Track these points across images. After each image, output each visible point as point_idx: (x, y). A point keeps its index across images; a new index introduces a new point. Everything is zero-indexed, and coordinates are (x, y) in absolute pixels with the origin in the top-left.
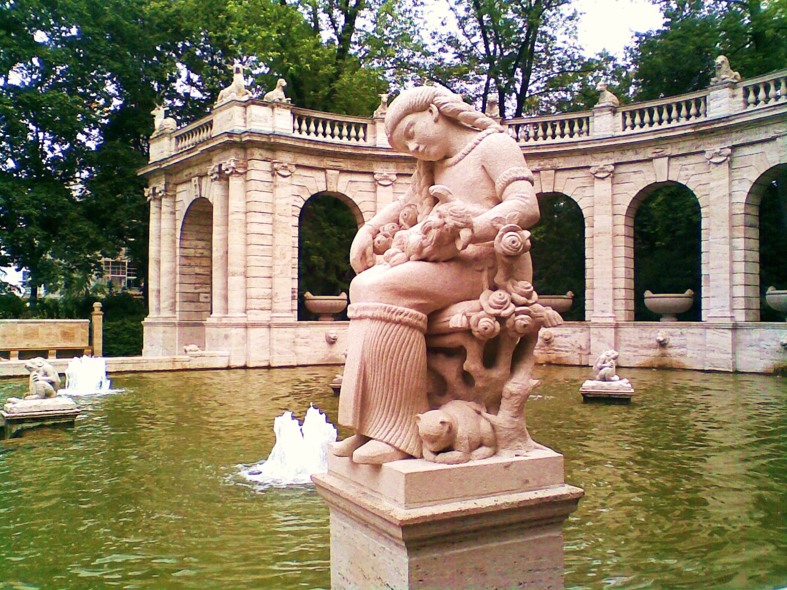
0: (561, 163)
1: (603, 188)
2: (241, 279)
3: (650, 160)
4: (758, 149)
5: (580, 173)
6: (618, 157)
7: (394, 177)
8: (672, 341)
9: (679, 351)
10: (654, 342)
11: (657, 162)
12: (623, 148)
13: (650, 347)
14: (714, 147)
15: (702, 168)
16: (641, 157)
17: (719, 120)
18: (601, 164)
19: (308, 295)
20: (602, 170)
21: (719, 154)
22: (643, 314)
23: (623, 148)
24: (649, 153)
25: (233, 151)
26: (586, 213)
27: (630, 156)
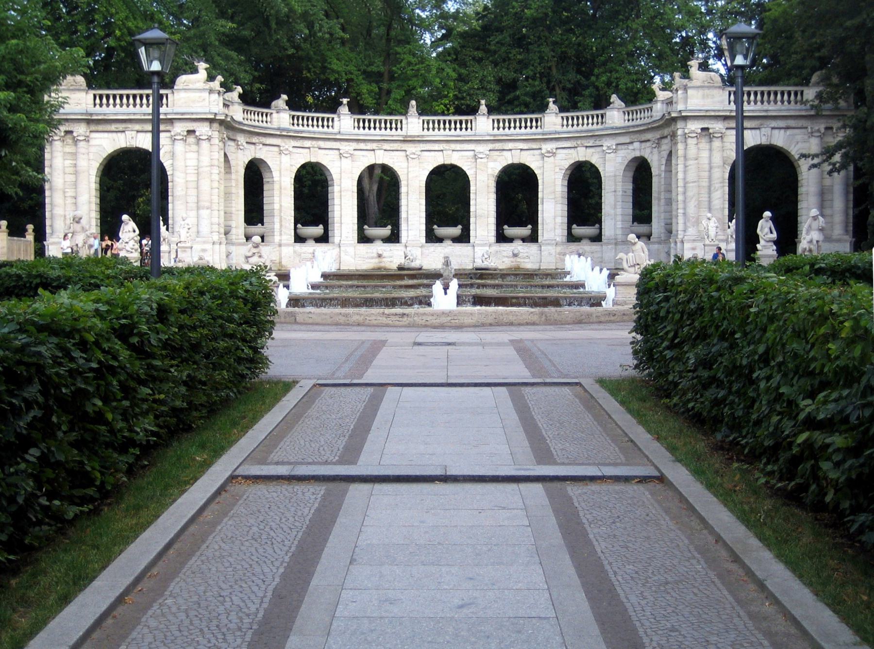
0: (322, 144)
1: (346, 163)
3: (374, 150)
6: (354, 145)
7: (244, 144)
8: (385, 254)
9: (389, 260)
10: (375, 255)
13: (372, 258)
14: (411, 148)
16: (368, 148)
17: (418, 136)
18: (347, 148)
19: (299, 226)
20: (347, 152)
21: (414, 154)
22: (363, 239)
23: (358, 141)
24: (374, 146)
26: (334, 177)
27: (362, 146)
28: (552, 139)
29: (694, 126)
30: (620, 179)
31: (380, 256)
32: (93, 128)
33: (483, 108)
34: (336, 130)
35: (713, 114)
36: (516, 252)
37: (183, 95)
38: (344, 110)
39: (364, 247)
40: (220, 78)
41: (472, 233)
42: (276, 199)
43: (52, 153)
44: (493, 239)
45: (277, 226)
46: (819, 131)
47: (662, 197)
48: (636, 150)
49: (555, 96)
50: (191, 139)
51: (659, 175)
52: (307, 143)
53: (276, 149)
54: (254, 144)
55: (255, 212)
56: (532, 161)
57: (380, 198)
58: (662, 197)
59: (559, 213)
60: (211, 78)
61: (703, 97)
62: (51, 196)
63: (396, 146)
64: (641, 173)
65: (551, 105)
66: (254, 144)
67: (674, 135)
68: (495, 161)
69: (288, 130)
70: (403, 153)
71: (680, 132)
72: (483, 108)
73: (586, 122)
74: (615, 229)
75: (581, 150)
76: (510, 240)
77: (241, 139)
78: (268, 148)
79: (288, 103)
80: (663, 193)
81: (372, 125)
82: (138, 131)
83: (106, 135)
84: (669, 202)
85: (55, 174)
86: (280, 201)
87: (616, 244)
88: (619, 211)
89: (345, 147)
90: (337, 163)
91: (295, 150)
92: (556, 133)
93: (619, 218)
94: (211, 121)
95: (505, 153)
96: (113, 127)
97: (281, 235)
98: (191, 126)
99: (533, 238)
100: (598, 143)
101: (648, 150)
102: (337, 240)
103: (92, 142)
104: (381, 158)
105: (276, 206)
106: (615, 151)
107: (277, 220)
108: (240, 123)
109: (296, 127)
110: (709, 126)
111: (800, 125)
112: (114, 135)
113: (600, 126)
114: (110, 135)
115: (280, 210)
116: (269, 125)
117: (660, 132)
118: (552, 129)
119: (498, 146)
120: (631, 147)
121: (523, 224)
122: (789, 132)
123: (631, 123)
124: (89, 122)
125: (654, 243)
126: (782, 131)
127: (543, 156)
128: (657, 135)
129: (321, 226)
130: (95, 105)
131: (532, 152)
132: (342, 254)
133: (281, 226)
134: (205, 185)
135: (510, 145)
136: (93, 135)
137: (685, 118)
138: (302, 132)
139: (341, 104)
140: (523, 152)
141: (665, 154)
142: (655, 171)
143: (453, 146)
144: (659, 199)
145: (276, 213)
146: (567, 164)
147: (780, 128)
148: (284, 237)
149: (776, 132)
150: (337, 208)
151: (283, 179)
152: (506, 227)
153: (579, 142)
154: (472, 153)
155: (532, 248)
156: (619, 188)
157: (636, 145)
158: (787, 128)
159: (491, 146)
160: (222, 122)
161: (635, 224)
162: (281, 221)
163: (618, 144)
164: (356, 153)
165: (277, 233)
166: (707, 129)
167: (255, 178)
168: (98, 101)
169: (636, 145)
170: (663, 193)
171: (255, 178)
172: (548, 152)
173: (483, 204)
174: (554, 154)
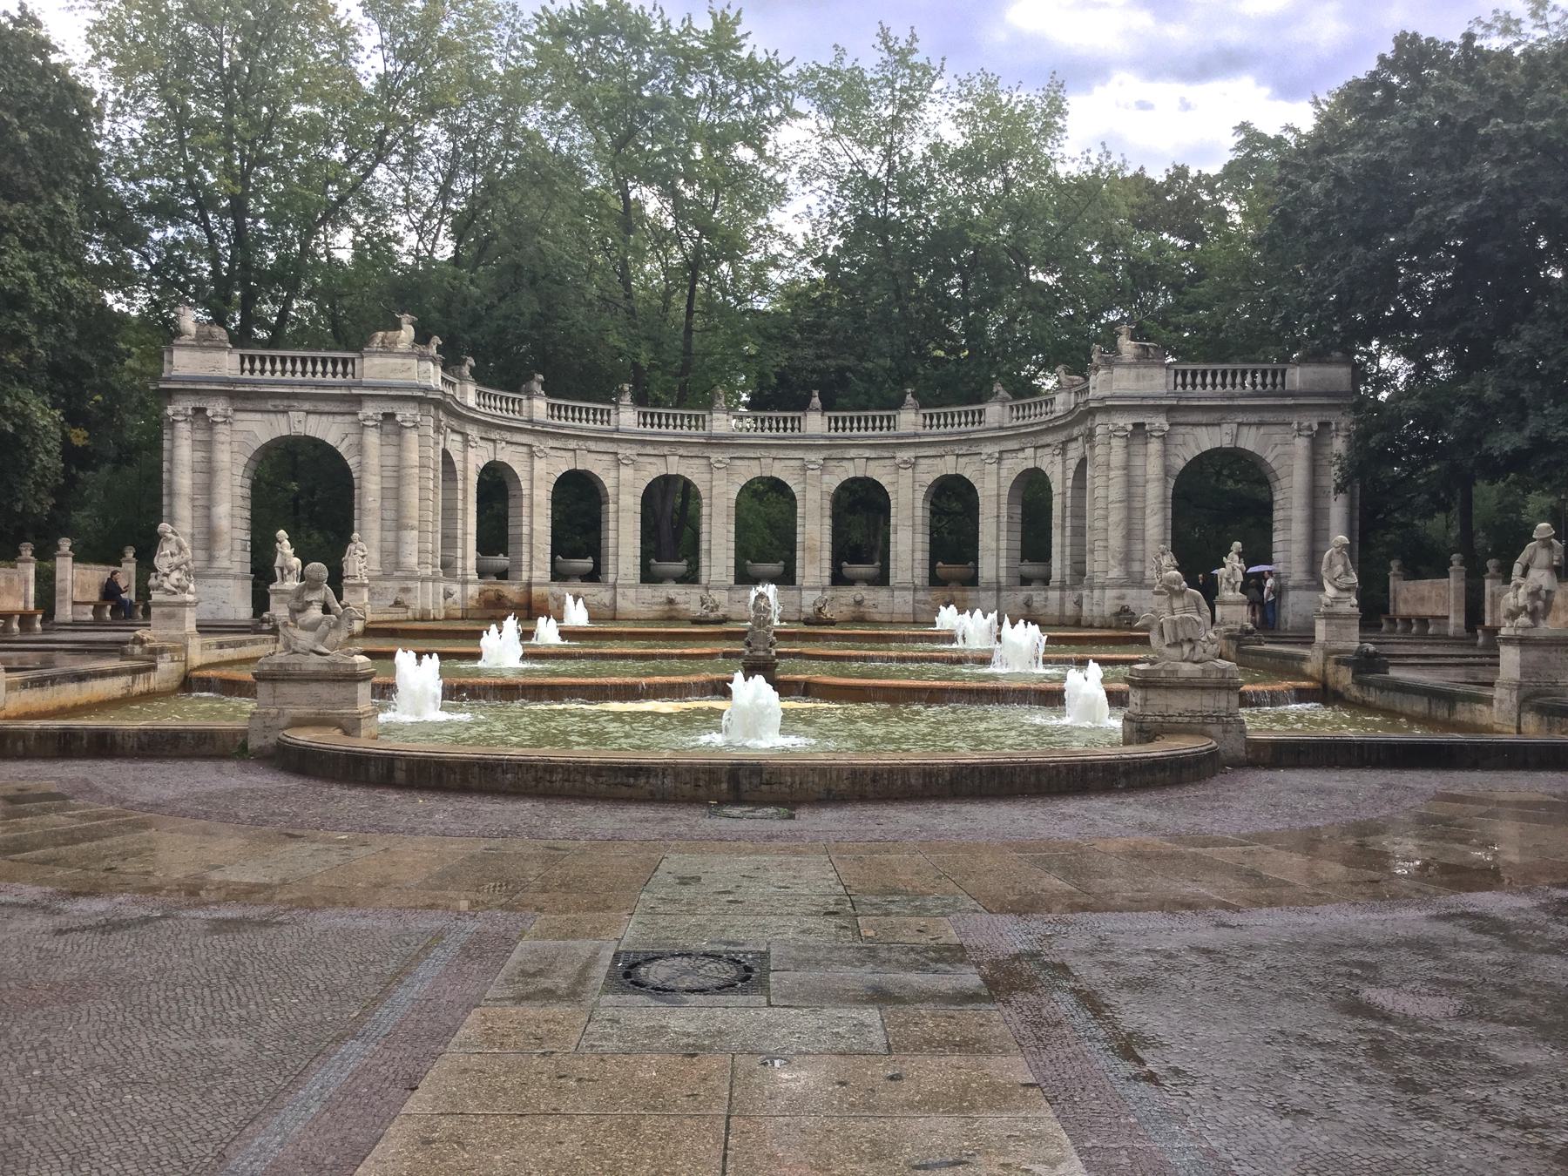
0: (592, 445)
2: (415, 533)
4: (746, 462)
5: (605, 457)
8: (678, 599)
11: (670, 459)
12: (643, 443)
14: (715, 455)
15: (703, 469)
18: (628, 452)
20: (627, 458)
23: (643, 443)
24: (666, 450)
25: (412, 405)
26: (610, 491)
27: (649, 450)
28: (909, 445)
29: (1126, 421)
30: (1004, 499)
31: (671, 601)
32: (239, 405)
33: (816, 401)
34: (612, 427)
35: (1152, 402)
36: (858, 598)
37: (377, 360)
38: (627, 399)
39: (648, 591)
40: (436, 340)
41: (799, 572)
42: (525, 520)
43: (172, 440)
44: (827, 581)
45: (525, 558)
46: (1310, 428)
47: (1068, 524)
48: (1026, 460)
49: (915, 384)
50: (388, 428)
51: (1064, 494)
52: (572, 444)
53: (525, 449)
54: (494, 441)
55: (496, 534)
56: (881, 473)
57: (671, 521)
58: (1068, 524)
59: (919, 546)
60: (422, 338)
61: (1138, 378)
62: (171, 505)
63: (695, 451)
64: (1032, 495)
65: (909, 397)
66: (494, 441)
67: (1090, 436)
68: (831, 473)
69: (545, 425)
70: (704, 462)
71: (1098, 430)
72: (816, 401)
73: (957, 422)
74: (998, 569)
75: (950, 459)
76: (851, 582)
77: (473, 432)
78: (513, 448)
79: (544, 386)
80: (1068, 519)
81: (664, 421)
82: (308, 413)
83: (258, 416)
84: (1079, 532)
85: (177, 471)
86: (531, 522)
87: (999, 590)
88: (1003, 544)
89: (625, 451)
90: (613, 474)
91: (553, 453)
92: (916, 435)
93: (1003, 553)
94: (420, 401)
95: (845, 463)
96: (270, 405)
97: (531, 570)
98: (388, 408)
99: (881, 579)
100: (974, 449)
101: (1047, 459)
102: (611, 578)
103: (238, 426)
104: (675, 466)
105: (525, 530)
106: (1000, 460)
107: (525, 548)
108: (470, 409)
109: (556, 421)
110: (1146, 421)
111: (1280, 420)
112: (272, 416)
113: (976, 427)
114: (266, 416)
115: (531, 536)
116: (517, 416)
117: (1065, 433)
118: (911, 430)
119: (836, 453)
120: (1021, 455)
121: (870, 561)
122: (1262, 430)
123: (1020, 422)
124: (232, 396)
125: (1053, 589)
126: (1254, 429)
127: (898, 467)
128: (1061, 436)
129: (590, 560)
130: (243, 371)
131: (882, 462)
132: (619, 599)
133: (532, 557)
134: (412, 494)
135: (852, 453)
136: (240, 416)
137: (1108, 410)
138: (563, 427)
139: (622, 392)
140: (871, 463)
141: (1072, 464)
142: (1056, 488)
143: (774, 453)
144: (1063, 528)
145: (525, 539)
146: (930, 479)
147: (1250, 425)
148: (536, 573)
149: (1245, 430)
150: (612, 534)
151: (535, 492)
152: (845, 564)
153: (948, 448)
154: (798, 463)
155: (881, 595)
156: (1004, 512)
157: (1029, 452)
158: (1260, 424)
159: (825, 454)
160: (438, 404)
161: (1026, 562)
162: (531, 552)
163: (1001, 452)
164: (641, 459)
165: (525, 568)
166: (1143, 424)
167: (497, 488)
168: (247, 365)
169: (1029, 452)
170: (1068, 519)
171: (497, 488)
172: (905, 462)
173: (814, 531)
174: (914, 465)
